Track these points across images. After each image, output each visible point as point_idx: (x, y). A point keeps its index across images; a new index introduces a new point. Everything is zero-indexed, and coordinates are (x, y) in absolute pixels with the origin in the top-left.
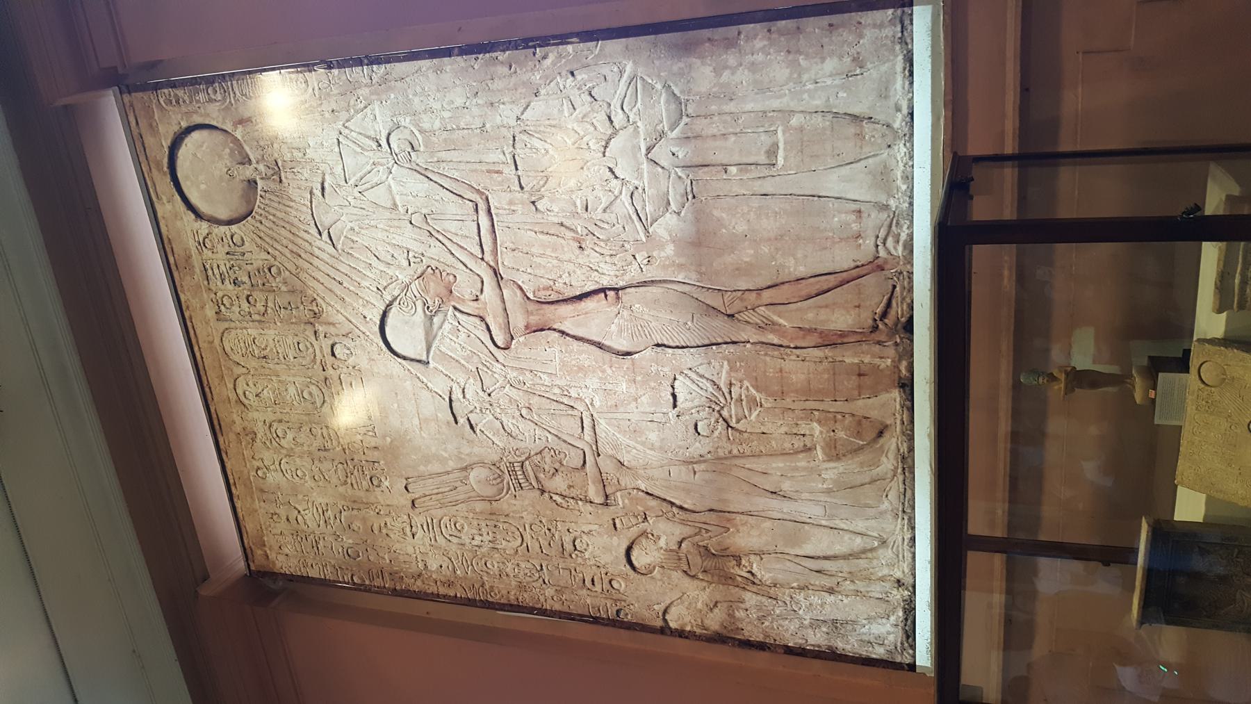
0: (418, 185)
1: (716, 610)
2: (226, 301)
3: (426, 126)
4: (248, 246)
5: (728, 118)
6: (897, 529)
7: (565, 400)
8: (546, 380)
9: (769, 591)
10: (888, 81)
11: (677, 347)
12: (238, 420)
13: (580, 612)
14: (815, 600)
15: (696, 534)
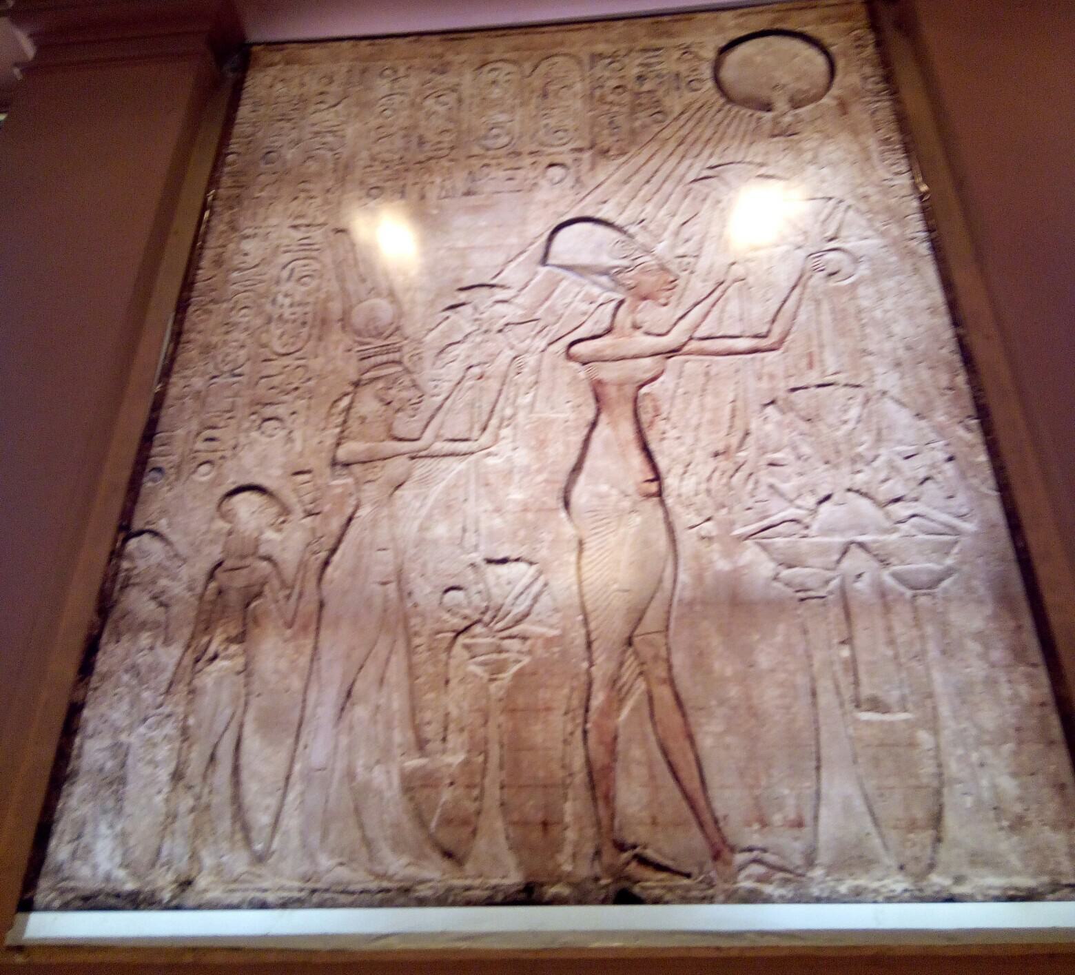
1: (152, 605)
3: (861, 291)
4: (689, 96)
6: (285, 875)
7: (494, 422)
9: (184, 682)
12: (463, 57)
14: (163, 752)
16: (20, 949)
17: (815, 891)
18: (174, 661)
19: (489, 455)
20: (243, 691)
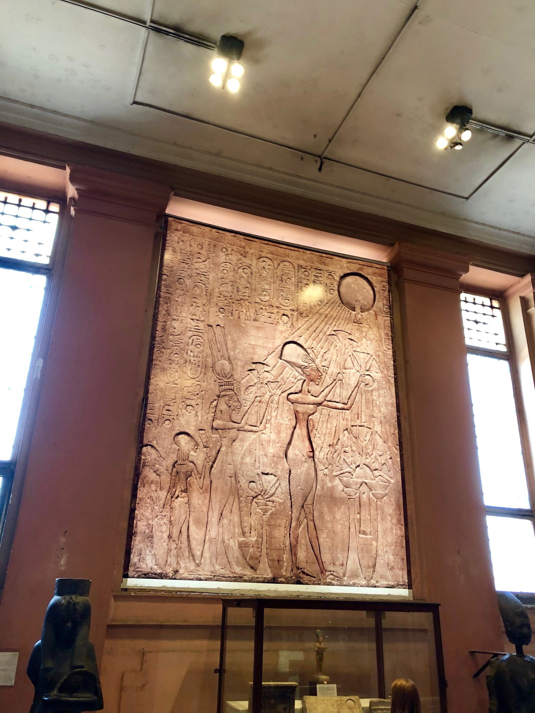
0: (353, 382)
1: (155, 474)
2: (306, 273)
3: (374, 392)
5: (376, 517)
6: (206, 571)
7: (264, 421)
8: (274, 414)
9: (168, 504)
10: (386, 579)
11: (289, 480)
12: (252, 251)
13: (150, 398)
14: (164, 528)
15: (198, 471)
16: (126, 590)
17: (345, 583)
18: (165, 496)
19: (263, 433)
20: (188, 510)
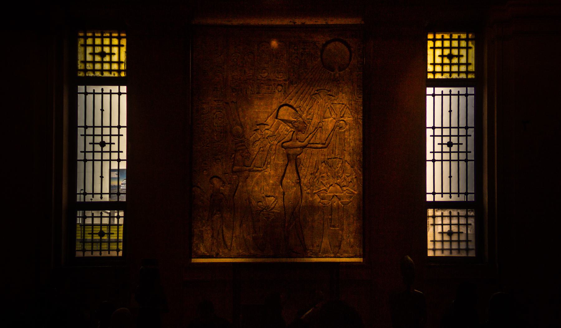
14: (209, 232)
